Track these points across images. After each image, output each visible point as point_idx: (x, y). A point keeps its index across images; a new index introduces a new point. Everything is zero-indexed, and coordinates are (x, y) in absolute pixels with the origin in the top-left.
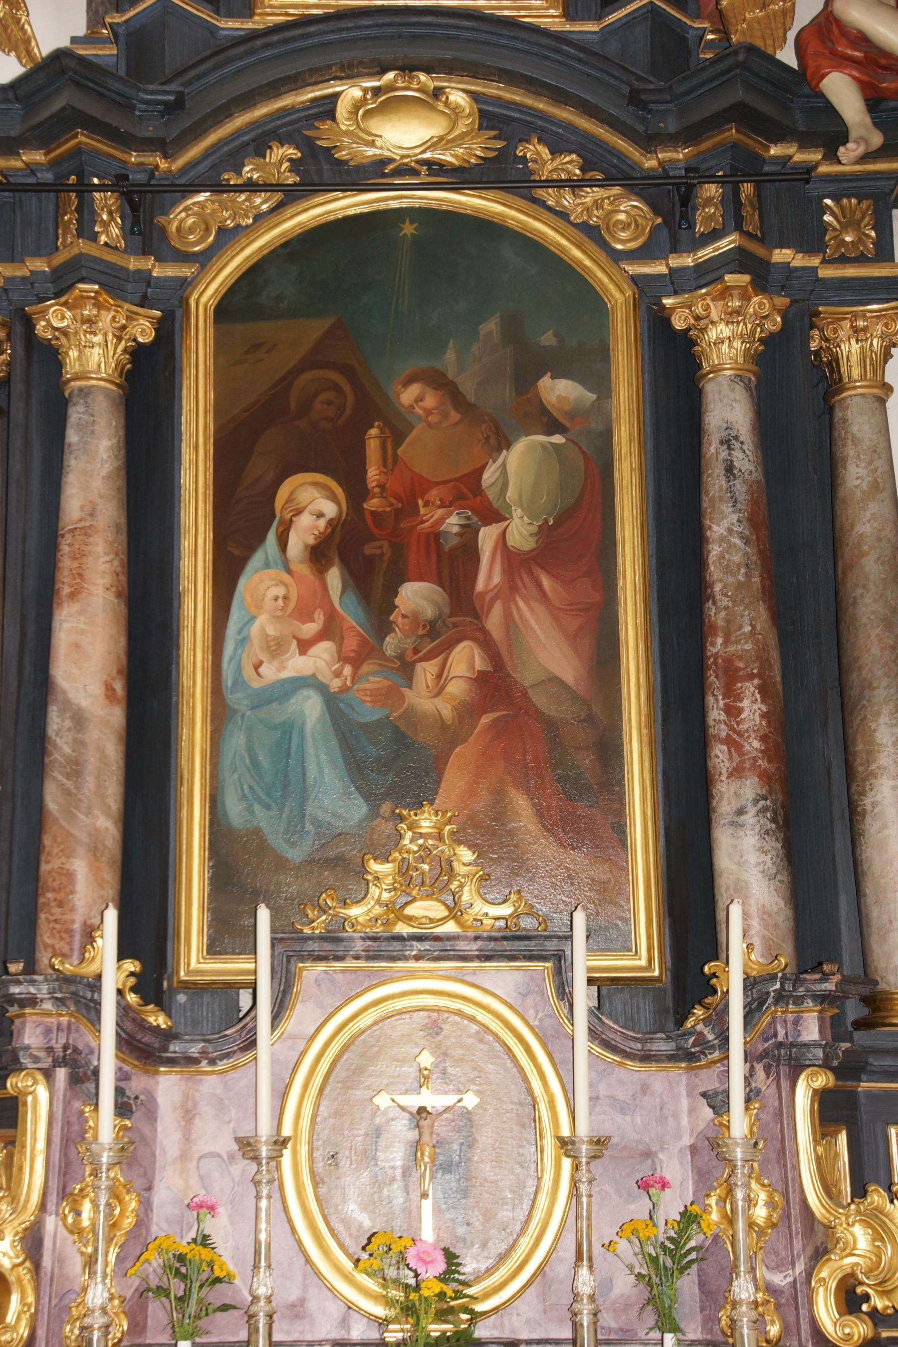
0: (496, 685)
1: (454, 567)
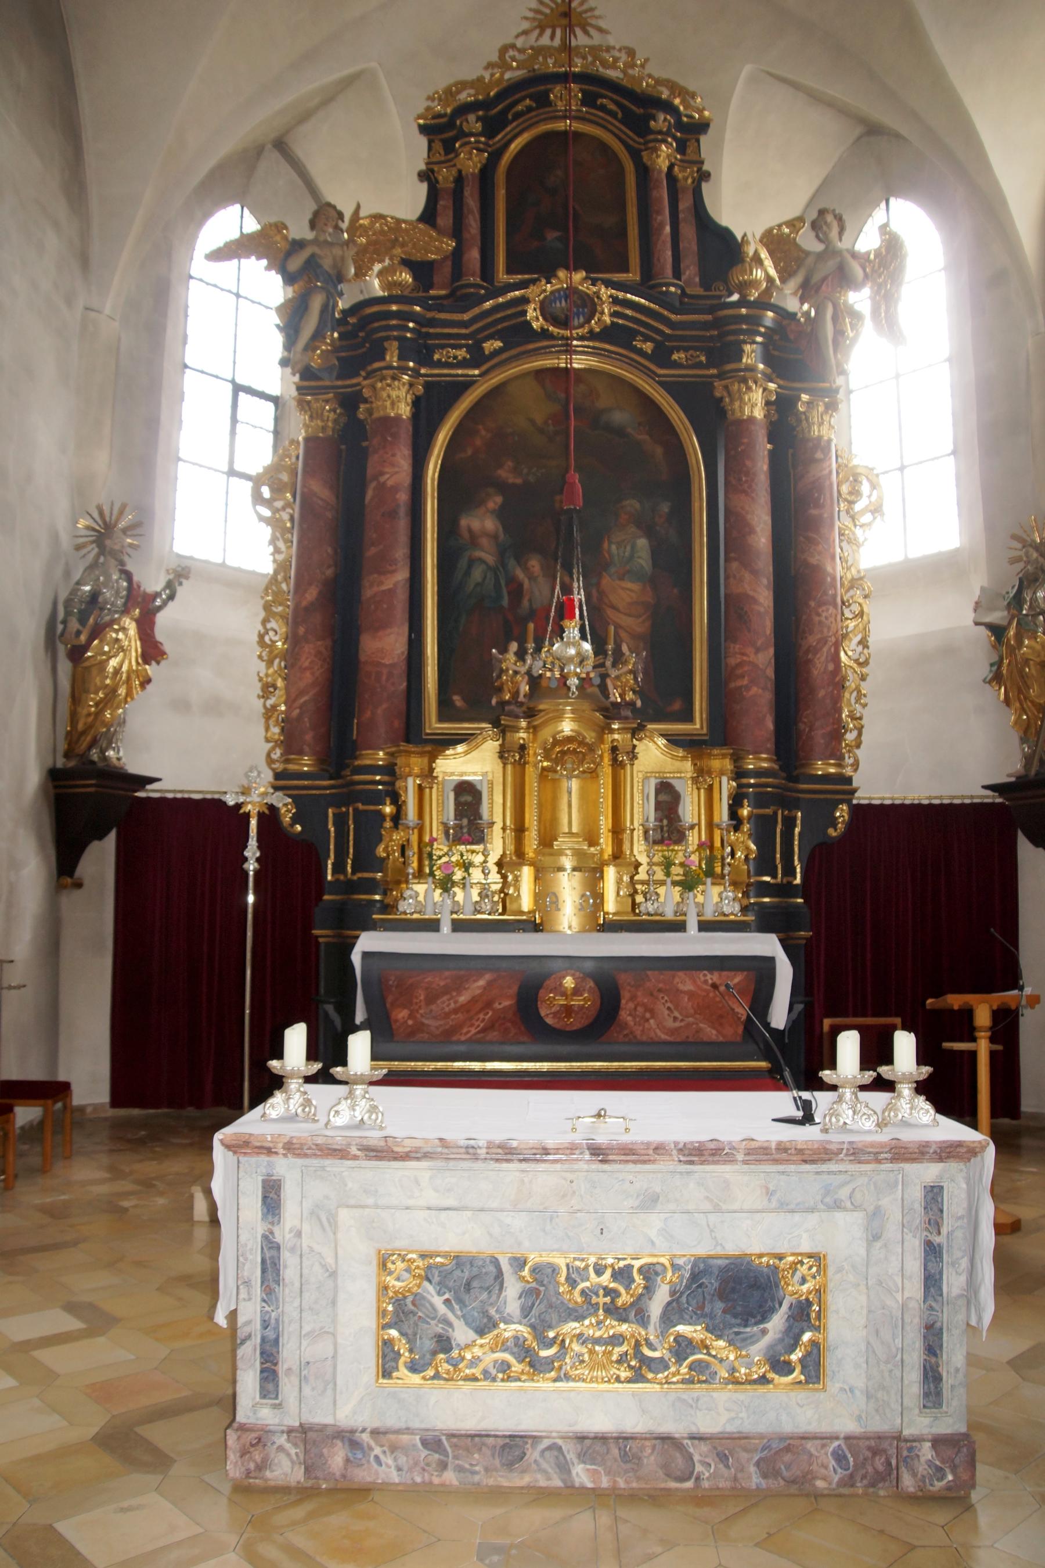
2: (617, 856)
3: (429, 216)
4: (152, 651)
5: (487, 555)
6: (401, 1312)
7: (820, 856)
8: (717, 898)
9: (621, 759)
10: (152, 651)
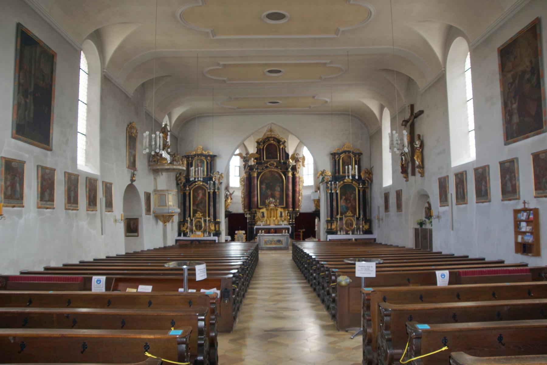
0: (352, 205)
1: (350, 200)
2: (277, 218)
3: (257, 153)
5: (264, 189)
7: (296, 218)
8: (286, 222)
9: (277, 210)
10: (231, 199)
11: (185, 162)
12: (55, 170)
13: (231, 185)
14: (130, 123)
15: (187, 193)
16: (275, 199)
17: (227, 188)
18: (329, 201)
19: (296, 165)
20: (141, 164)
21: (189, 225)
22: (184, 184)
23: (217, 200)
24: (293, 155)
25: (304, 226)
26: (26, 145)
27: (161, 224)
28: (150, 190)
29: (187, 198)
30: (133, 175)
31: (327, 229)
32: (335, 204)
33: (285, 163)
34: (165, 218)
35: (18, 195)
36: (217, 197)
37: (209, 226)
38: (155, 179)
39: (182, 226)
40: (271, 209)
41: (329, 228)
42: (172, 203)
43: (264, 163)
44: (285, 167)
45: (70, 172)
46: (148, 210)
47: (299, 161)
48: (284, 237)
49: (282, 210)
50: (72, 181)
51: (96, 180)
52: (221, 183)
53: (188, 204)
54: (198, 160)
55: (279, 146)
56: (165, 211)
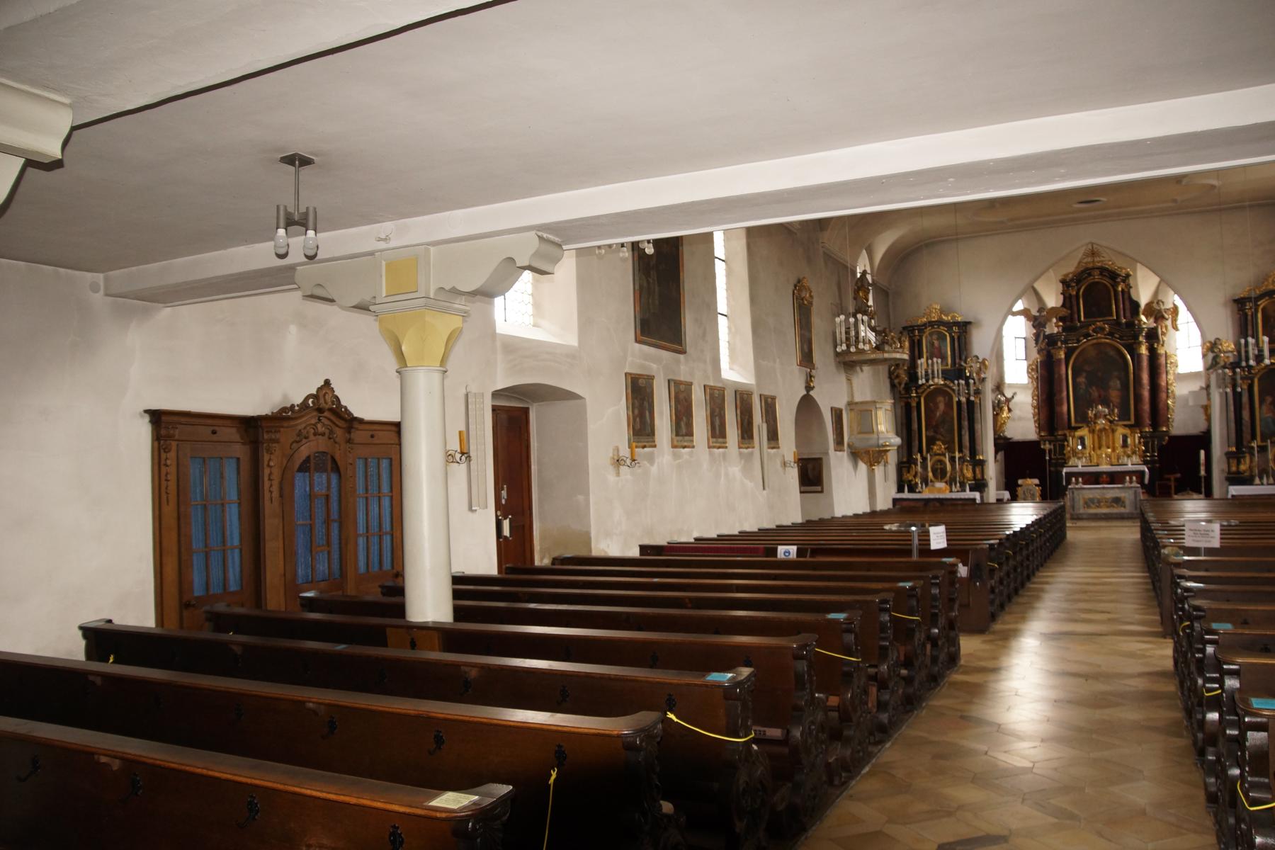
2: (1114, 450)
3: (1063, 305)
4: (1010, 410)
5: (1083, 387)
6: (1086, 503)
9: (1113, 431)
10: (1010, 410)
11: (907, 344)
12: (691, 384)
13: (1010, 378)
14: (799, 281)
15: (914, 404)
16: (1108, 407)
17: (999, 388)
18: (1232, 408)
19: (1155, 329)
20: (822, 355)
21: (919, 469)
22: (904, 386)
23: (977, 415)
24: (1149, 305)
25: (1176, 465)
26: (652, 350)
27: (863, 467)
28: (841, 404)
29: (915, 414)
30: (810, 378)
31: (1229, 472)
32: (1246, 415)
33: (1130, 325)
34: (870, 455)
35: (648, 429)
36: (977, 410)
37: (961, 470)
38: (849, 380)
39: (904, 470)
40: (1101, 431)
41: (1234, 469)
42: (884, 426)
43: (1081, 327)
44: (1130, 333)
45: (712, 384)
46: (839, 442)
47: (1163, 318)
48: (1128, 493)
49: (1127, 431)
50: (716, 398)
51: (750, 394)
52: (984, 380)
53: (915, 426)
54: (931, 334)
55: (1115, 286)
56: (873, 442)
